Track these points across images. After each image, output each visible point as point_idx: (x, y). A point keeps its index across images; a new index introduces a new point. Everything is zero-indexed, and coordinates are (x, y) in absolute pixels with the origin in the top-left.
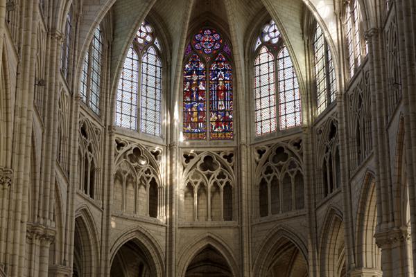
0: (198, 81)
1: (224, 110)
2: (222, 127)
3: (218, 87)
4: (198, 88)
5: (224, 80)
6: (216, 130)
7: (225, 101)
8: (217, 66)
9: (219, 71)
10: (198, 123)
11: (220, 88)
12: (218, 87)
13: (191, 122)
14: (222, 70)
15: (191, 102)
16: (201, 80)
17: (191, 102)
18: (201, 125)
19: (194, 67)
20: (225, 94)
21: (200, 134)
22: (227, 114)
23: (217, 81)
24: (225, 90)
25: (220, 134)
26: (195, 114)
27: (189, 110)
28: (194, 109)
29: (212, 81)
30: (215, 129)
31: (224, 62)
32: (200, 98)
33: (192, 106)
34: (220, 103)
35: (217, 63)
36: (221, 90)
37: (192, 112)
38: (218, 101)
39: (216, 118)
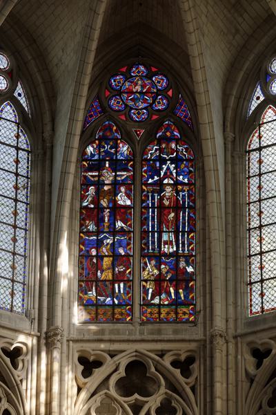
0: (116, 185)
1: (175, 254)
2: (169, 294)
3: (161, 199)
4: (115, 202)
5: (177, 183)
6: (156, 301)
7: (176, 233)
8: (161, 150)
9: (163, 161)
10: (113, 282)
11: (166, 203)
12: (161, 199)
13: (97, 280)
14: (173, 161)
15: (98, 233)
16: (123, 183)
17: (98, 233)
18: (120, 287)
19: (106, 152)
20: (177, 217)
21: (117, 310)
22: (182, 264)
23: (160, 186)
24: (177, 207)
25: (164, 311)
26: (107, 262)
27: (94, 252)
28: (104, 250)
29: (147, 185)
30: (152, 299)
31: (177, 141)
32: (119, 224)
33: (99, 244)
34: (165, 237)
35: (159, 144)
36: (169, 207)
37: (100, 257)
38: (160, 233)
39: (156, 272)
